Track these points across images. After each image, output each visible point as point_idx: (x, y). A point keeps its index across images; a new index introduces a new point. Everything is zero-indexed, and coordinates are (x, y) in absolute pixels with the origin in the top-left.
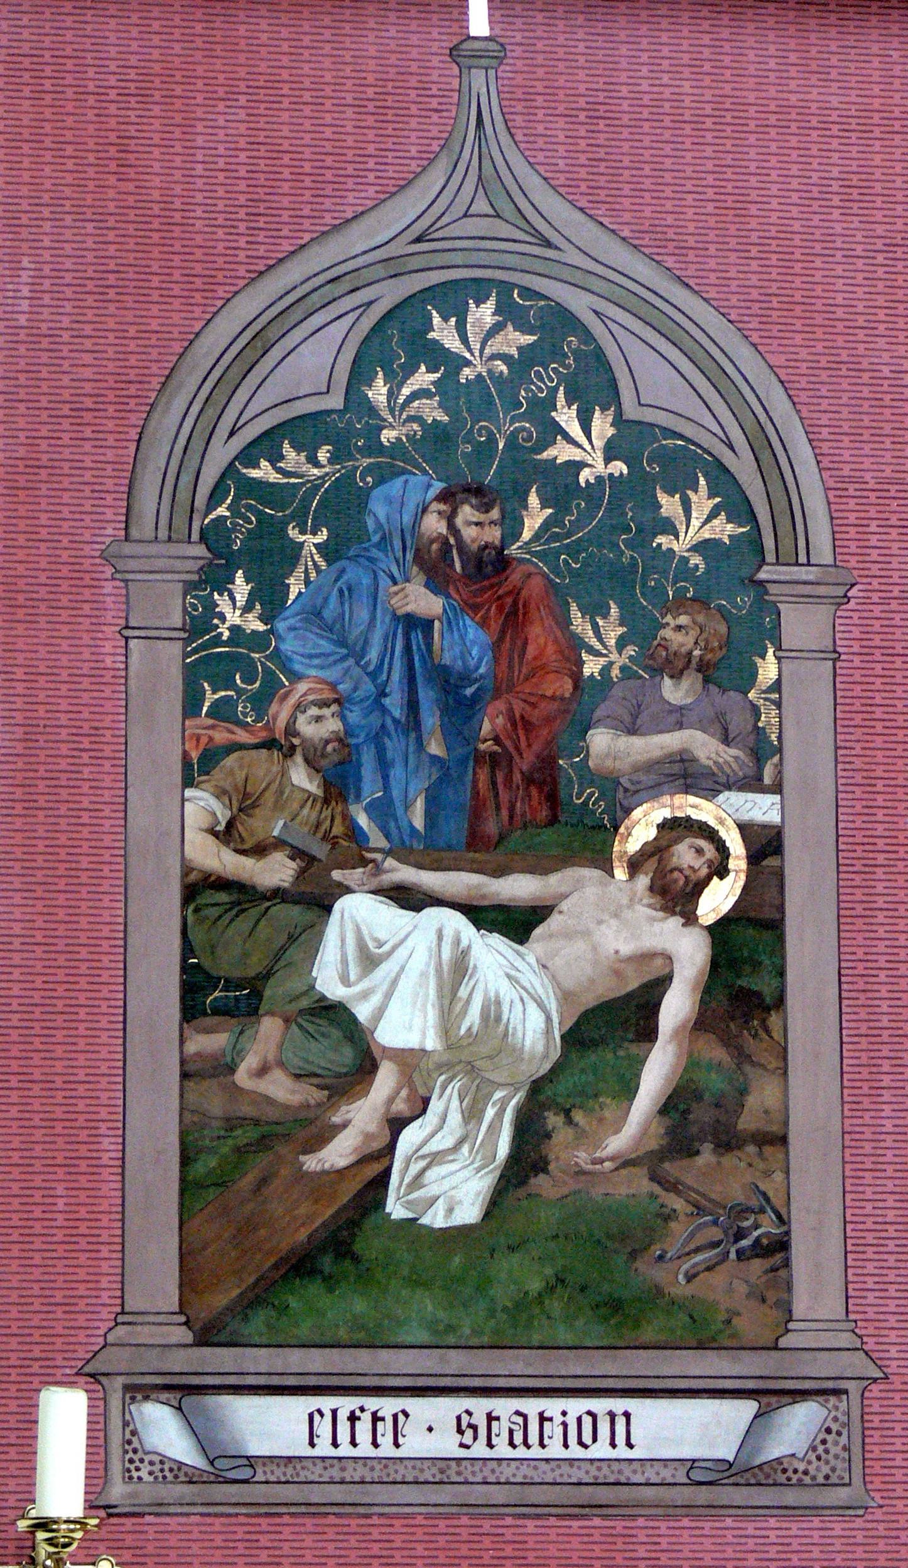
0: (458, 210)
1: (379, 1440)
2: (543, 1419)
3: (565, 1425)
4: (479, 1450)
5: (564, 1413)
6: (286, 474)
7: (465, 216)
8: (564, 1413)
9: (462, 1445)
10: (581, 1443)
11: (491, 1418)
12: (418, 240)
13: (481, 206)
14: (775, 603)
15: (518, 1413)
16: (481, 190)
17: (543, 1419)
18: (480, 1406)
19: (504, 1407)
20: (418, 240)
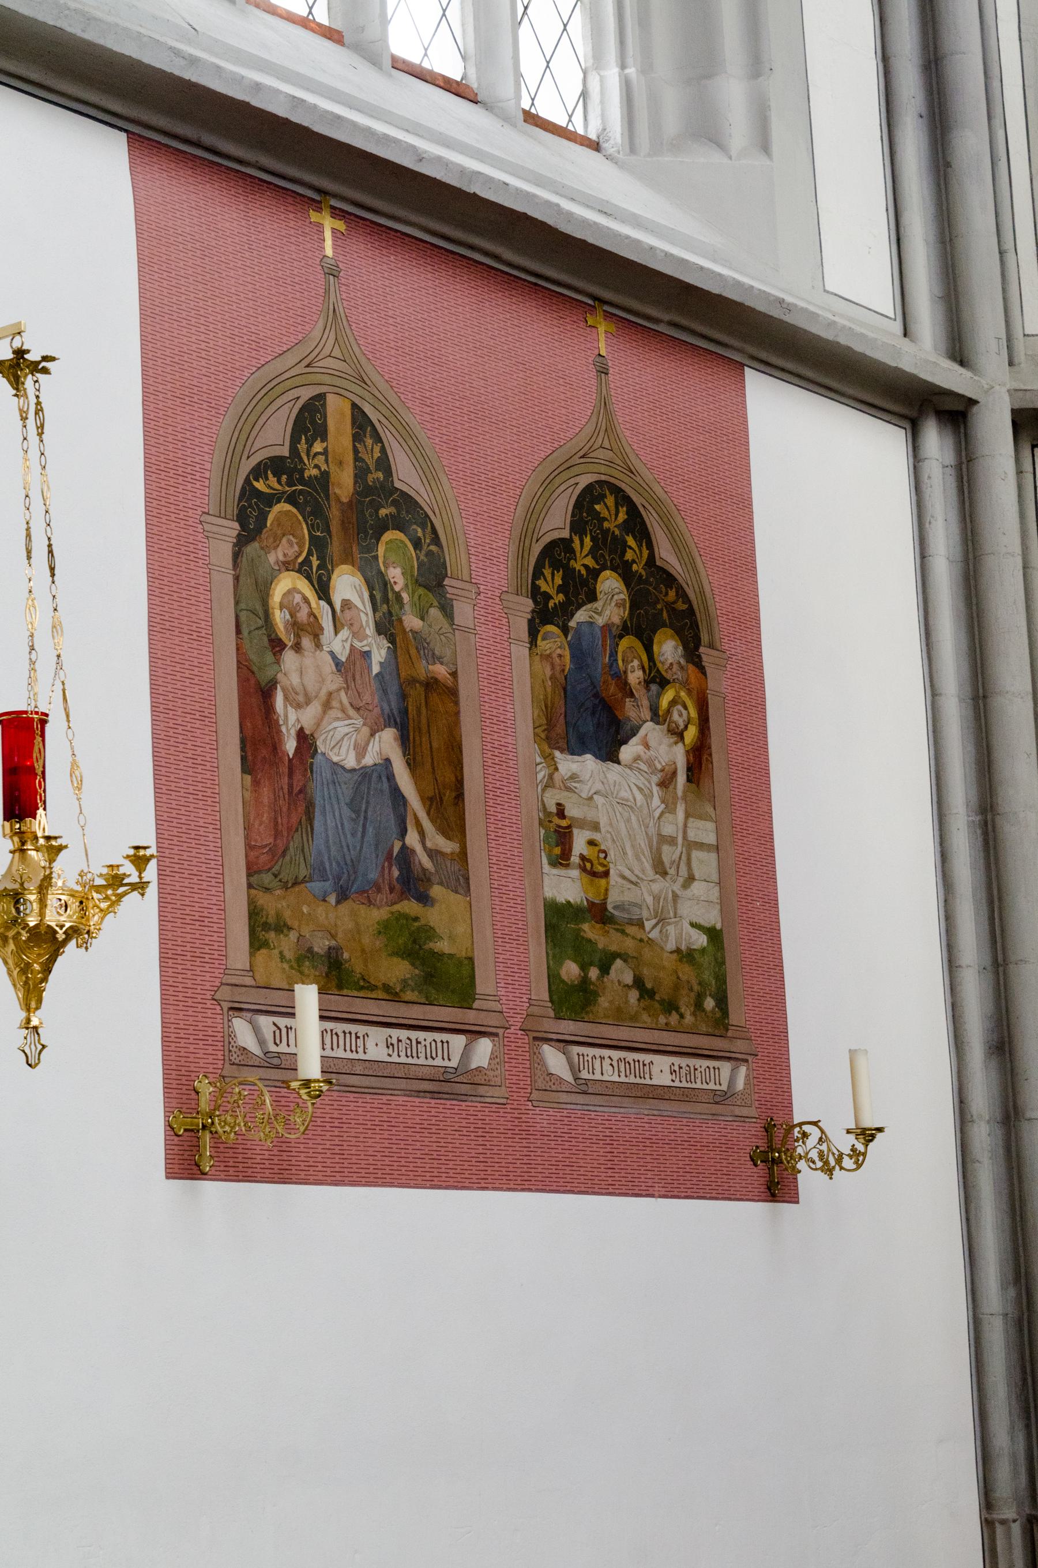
0: (326, 351)
1: (400, 1053)
2: (418, 1043)
3: (425, 1046)
4: (395, 1059)
5: (425, 1040)
6: (269, 487)
7: (330, 356)
8: (425, 1040)
9: (389, 1055)
10: (432, 1057)
11: (399, 1041)
12: (308, 366)
13: (337, 353)
14: (452, 600)
15: (408, 1038)
16: (337, 344)
17: (418, 1043)
18: (396, 1033)
19: (404, 1034)
20: (308, 366)
